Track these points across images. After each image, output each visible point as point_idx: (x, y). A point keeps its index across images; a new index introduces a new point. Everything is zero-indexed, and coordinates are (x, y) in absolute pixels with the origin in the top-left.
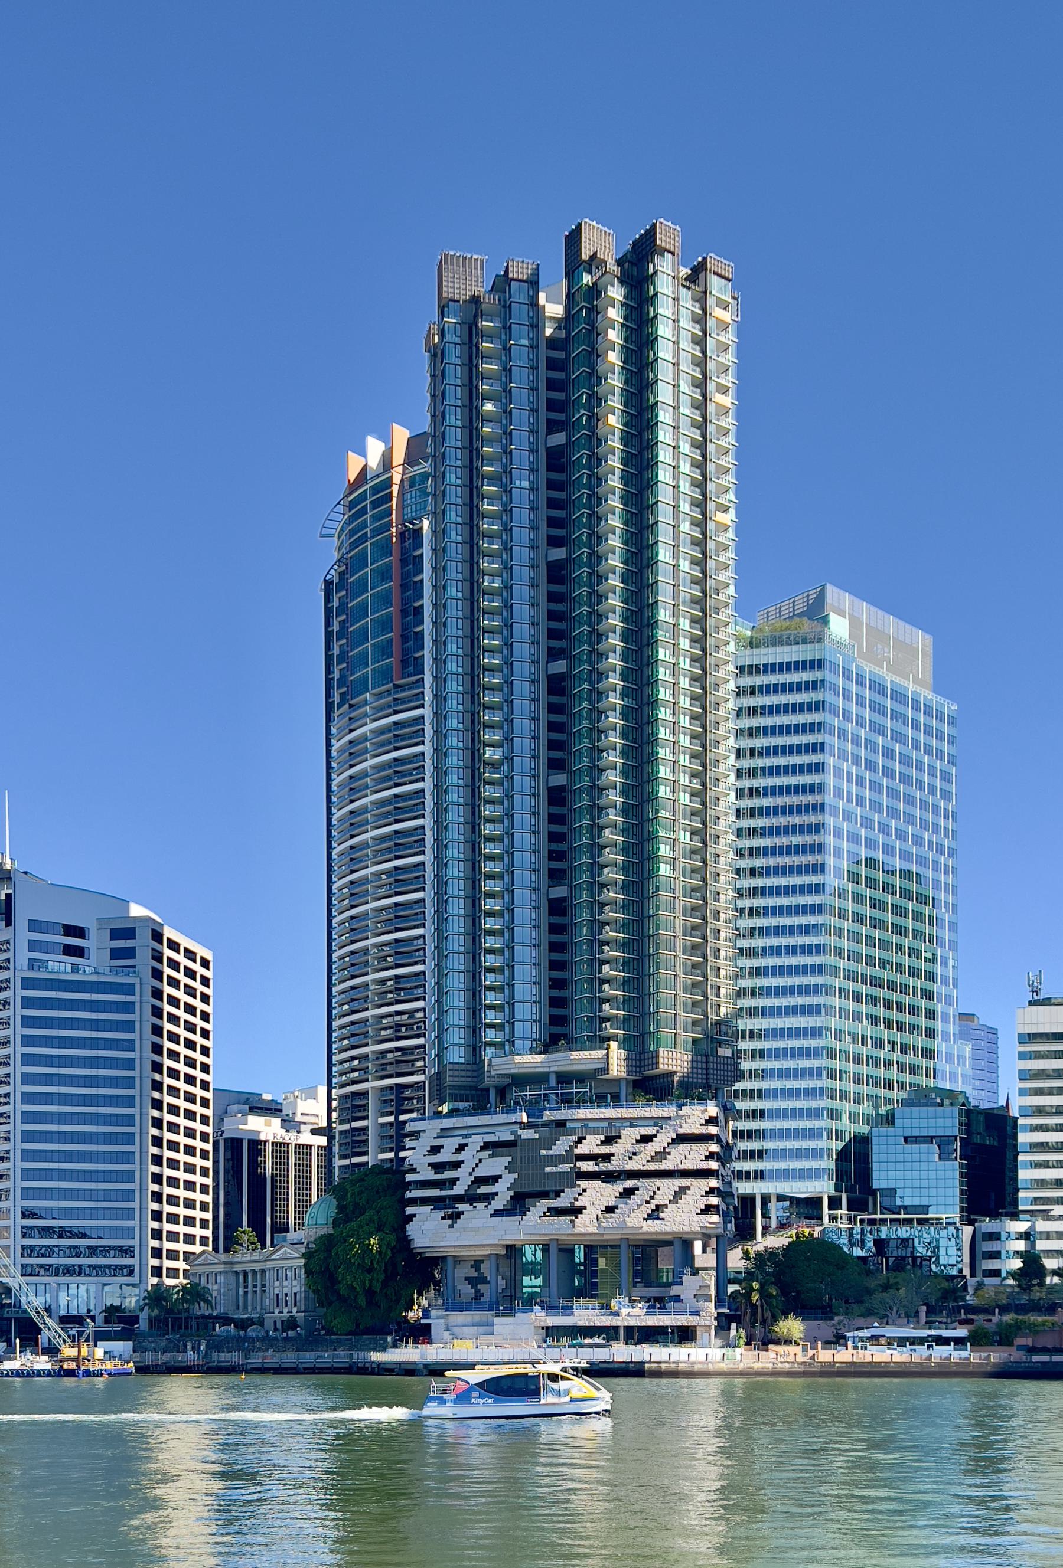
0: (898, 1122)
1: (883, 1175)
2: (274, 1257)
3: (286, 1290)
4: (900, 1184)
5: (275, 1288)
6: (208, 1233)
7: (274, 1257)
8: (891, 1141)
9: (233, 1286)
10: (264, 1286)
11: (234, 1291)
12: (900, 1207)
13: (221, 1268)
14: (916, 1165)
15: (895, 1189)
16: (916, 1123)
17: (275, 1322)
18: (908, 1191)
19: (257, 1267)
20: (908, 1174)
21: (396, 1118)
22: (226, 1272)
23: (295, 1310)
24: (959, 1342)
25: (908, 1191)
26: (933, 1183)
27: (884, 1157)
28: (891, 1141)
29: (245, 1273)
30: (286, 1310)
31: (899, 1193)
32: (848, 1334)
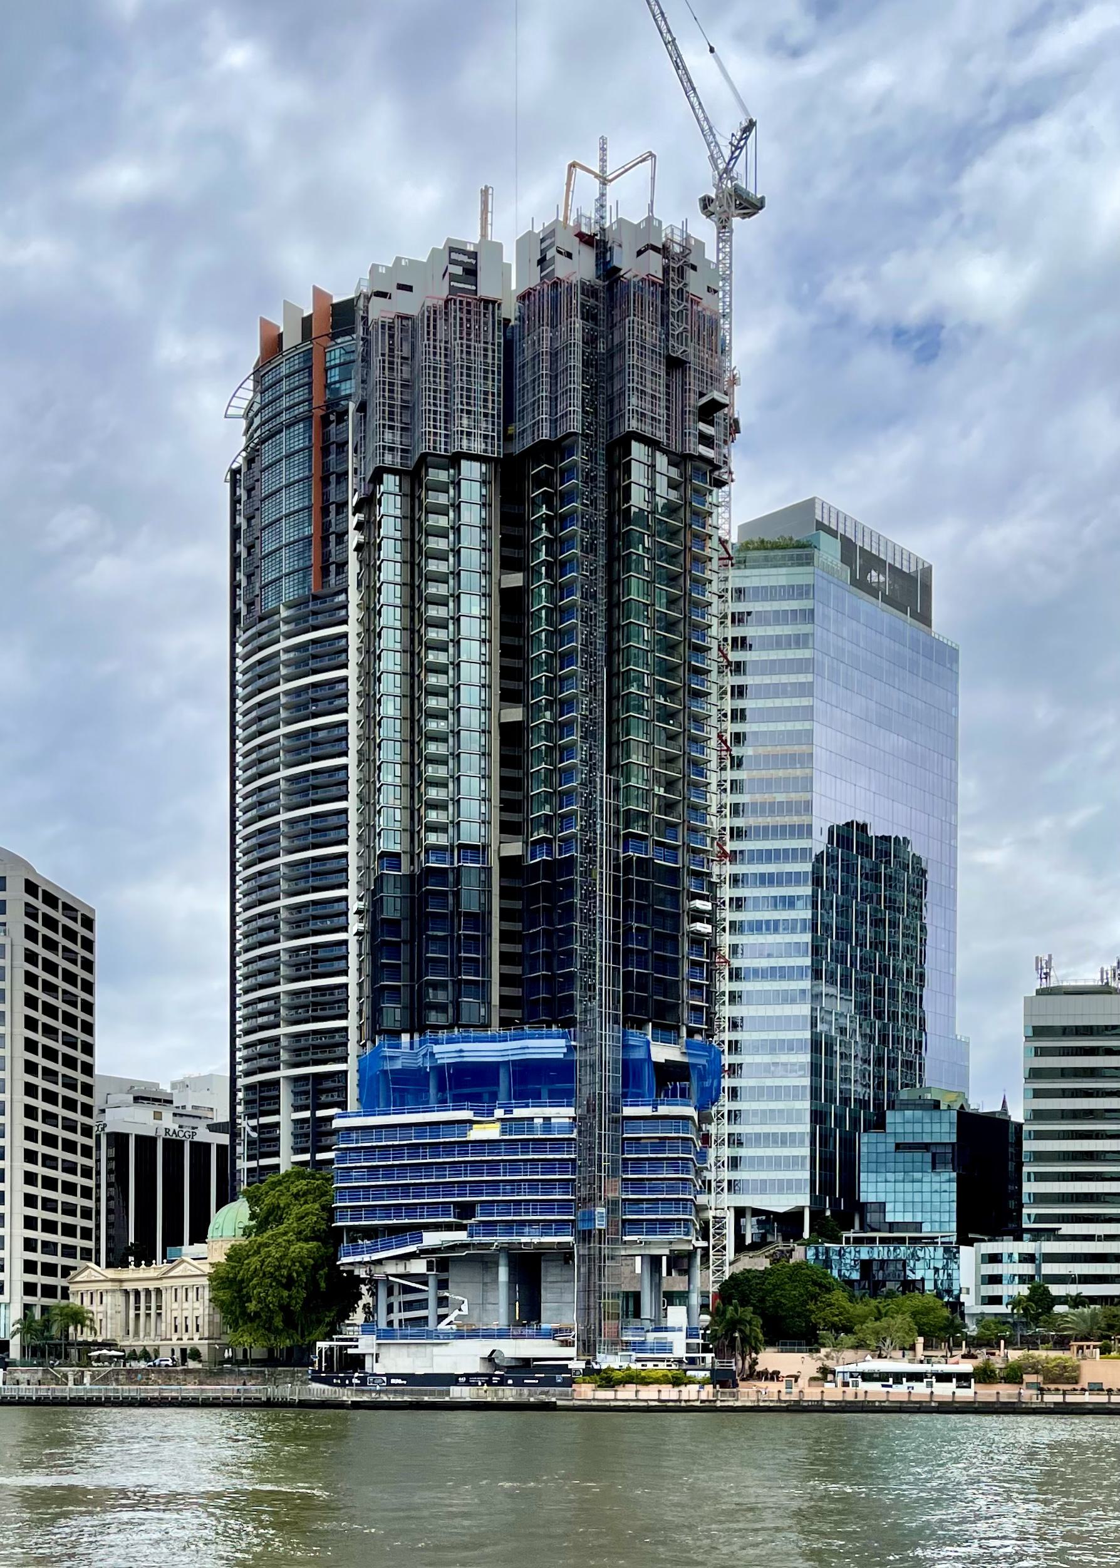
1: (872, 1187)
2: (171, 1274)
3: (185, 1314)
5: (172, 1308)
7: (171, 1274)
9: (122, 1308)
10: (159, 1307)
11: (123, 1314)
12: (890, 1224)
13: (108, 1286)
15: (884, 1203)
16: (909, 1128)
17: (173, 1351)
18: (899, 1206)
19: (151, 1286)
20: (900, 1186)
21: (313, 1114)
22: (114, 1291)
23: (196, 1336)
29: (137, 1293)
30: (185, 1337)
31: (889, 1207)
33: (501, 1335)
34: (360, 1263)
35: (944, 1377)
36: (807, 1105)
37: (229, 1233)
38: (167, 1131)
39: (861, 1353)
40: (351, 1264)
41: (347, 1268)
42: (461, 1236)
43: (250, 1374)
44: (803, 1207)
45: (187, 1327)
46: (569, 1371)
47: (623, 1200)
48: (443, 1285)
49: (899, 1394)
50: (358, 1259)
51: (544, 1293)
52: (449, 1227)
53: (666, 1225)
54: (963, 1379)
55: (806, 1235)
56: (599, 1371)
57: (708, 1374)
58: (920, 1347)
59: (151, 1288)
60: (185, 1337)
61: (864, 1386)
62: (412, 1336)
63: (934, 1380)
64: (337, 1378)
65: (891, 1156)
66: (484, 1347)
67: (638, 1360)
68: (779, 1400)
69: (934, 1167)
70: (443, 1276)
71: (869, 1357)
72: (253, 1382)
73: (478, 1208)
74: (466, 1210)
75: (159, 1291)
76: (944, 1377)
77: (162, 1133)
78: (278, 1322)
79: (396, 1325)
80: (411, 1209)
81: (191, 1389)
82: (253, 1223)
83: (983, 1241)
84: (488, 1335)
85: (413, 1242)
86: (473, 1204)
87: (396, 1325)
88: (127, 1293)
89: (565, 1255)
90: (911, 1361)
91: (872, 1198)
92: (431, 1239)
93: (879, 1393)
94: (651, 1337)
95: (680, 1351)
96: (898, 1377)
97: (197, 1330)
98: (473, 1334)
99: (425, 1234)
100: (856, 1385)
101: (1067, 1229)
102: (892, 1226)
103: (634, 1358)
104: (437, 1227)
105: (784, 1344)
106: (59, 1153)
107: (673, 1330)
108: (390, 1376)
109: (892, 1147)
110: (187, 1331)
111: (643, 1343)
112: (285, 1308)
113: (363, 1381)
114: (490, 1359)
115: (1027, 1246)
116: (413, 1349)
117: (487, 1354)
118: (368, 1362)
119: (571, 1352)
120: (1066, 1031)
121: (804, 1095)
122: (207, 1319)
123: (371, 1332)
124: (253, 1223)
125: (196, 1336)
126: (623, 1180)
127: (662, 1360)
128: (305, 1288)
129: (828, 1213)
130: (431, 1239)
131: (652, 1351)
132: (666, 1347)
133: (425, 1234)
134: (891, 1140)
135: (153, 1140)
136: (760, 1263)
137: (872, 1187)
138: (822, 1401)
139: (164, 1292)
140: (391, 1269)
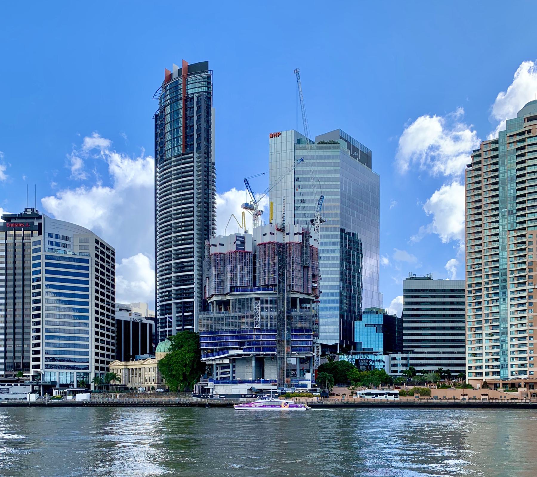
0: (363, 319)
1: (358, 337)
3: (149, 376)
4: (363, 341)
5: (146, 375)
6: (114, 354)
8: (361, 326)
13: (123, 367)
14: (369, 334)
18: (366, 343)
19: (137, 367)
22: (124, 369)
23: (153, 383)
24: (396, 395)
25: (366, 343)
26: (375, 340)
27: (358, 331)
28: (361, 326)
29: (132, 369)
30: (149, 383)
31: (363, 343)
32: (358, 392)
33: (254, 382)
34: (208, 360)
35: (390, 395)
36: (338, 313)
37: (163, 350)
38: (133, 319)
39: (364, 387)
40: (205, 360)
41: (203, 362)
42: (241, 352)
43: (172, 394)
44: (337, 344)
45: (150, 380)
46: (277, 393)
47: (292, 341)
48: (234, 367)
49: (378, 399)
50: (208, 358)
51: (265, 369)
52: (237, 349)
53: (305, 349)
54: (396, 395)
55: (338, 352)
56: (285, 393)
57: (319, 394)
58: (380, 385)
59: (137, 368)
60: (149, 383)
61: (366, 397)
62: (225, 383)
64: (202, 396)
65: (363, 328)
66: (249, 386)
67: (297, 390)
68: (342, 402)
69: (376, 332)
70: (234, 364)
71: (367, 389)
72: (173, 397)
73: (246, 343)
74: (242, 344)
75: (140, 369)
76: (390, 395)
77: (132, 320)
78: (181, 378)
79: (219, 379)
80: (225, 344)
81: (153, 400)
82: (172, 347)
83: (391, 354)
84: (249, 382)
85: (225, 354)
86: (244, 342)
87: (219, 379)
88: (129, 369)
89: (273, 357)
90: (379, 390)
91: (358, 341)
92: (231, 353)
93: (371, 399)
94: (300, 383)
95: (309, 387)
96: (376, 395)
97: (153, 381)
98: (245, 382)
99: (229, 351)
100: (364, 397)
101: (416, 350)
102: (364, 349)
103: (295, 389)
104: (233, 349)
105: (339, 385)
106: (105, 325)
107: (307, 380)
108: (220, 395)
109: (364, 325)
110: (150, 381)
111: (298, 384)
112: (184, 375)
113: (211, 397)
114: (251, 390)
115: (404, 355)
116: (225, 387)
117: (249, 388)
118: (211, 390)
119: (276, 387)
120: (416, 291)
121: (337, 309)
122: (157, 377)
123: (212, 381)
124: (172, 347)
125: (153, 383)
126: (292, 334)
127: (305, 390)
128: (190, 367)
129: (344, 346)
130: (231, 353)
131: (301, 387)
132: (306, 386)
133: (229, 351)
134: (364, 323)
135: (129, 322)
136: (326, 361)
137: (358, 337)
138: (355, 402)
139: (142, 369)
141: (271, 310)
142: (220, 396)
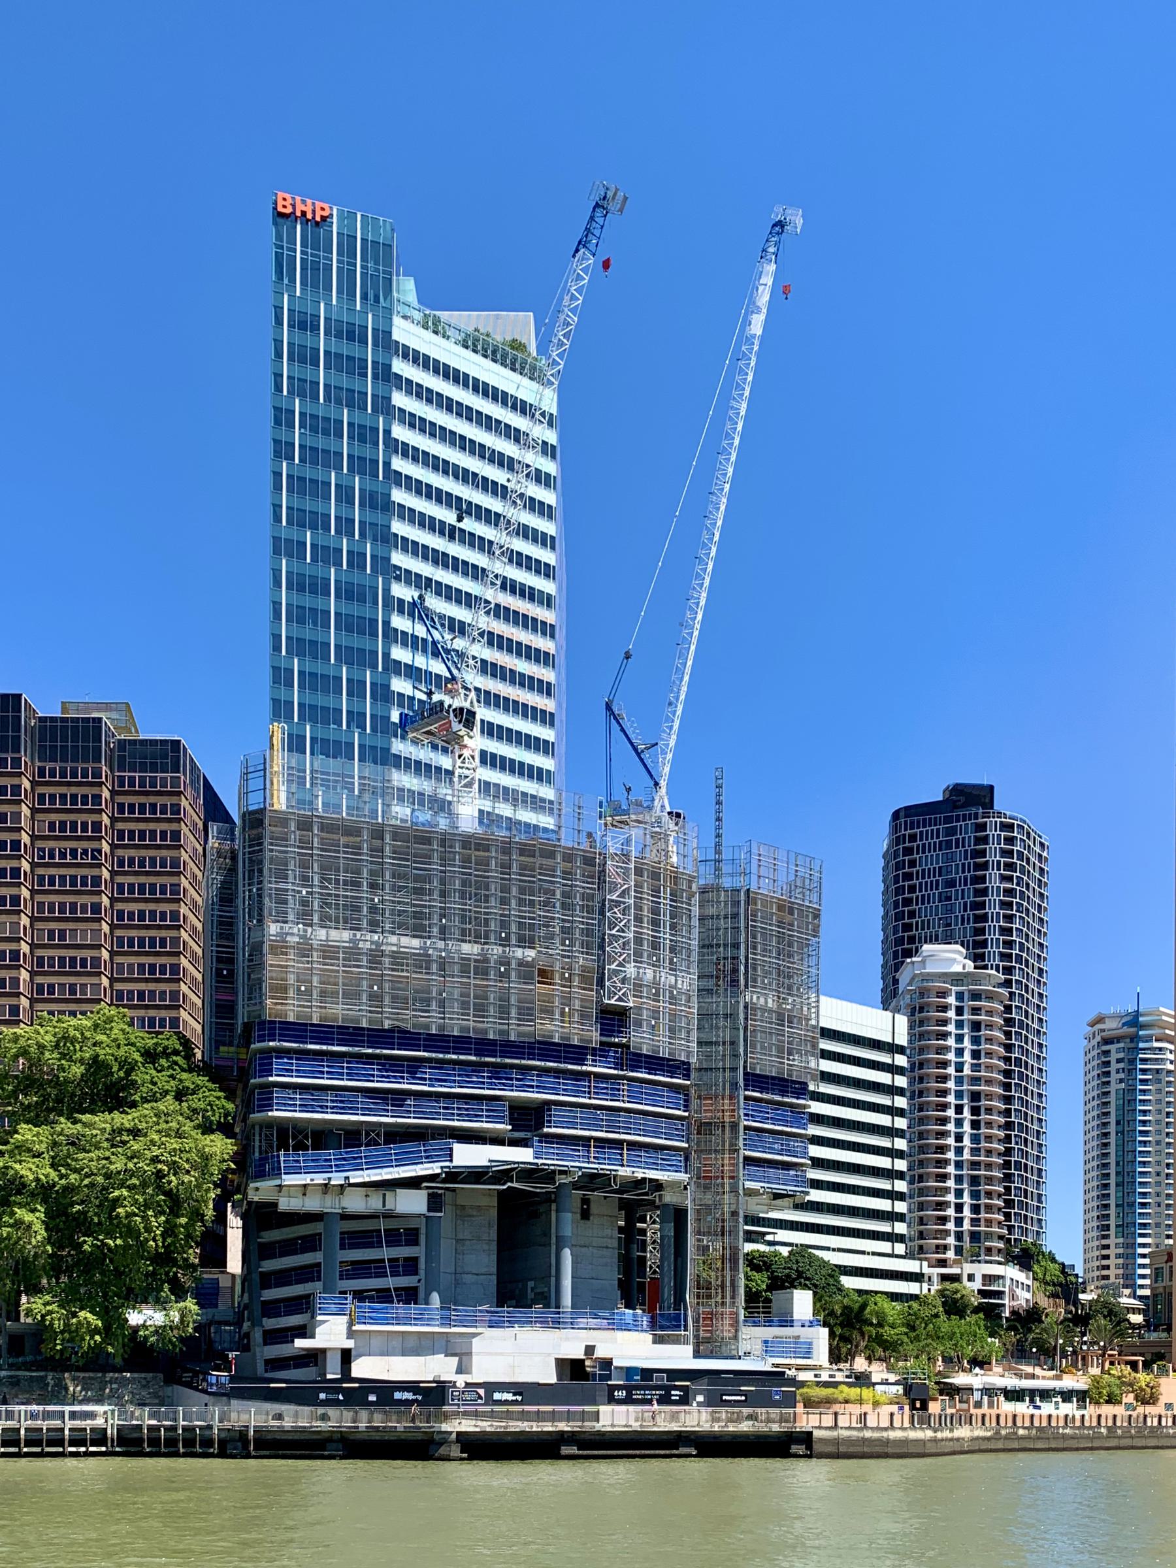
42: (523, 1155)
54: (1082, 1397)
63: (1059, 1399)
85: (430, 1158)
92: (467, 1155)
108: (492, 1387)
130: (467, 1155)
140: (355, 1203)
141: (671, 962)
142: (489, 1395)
